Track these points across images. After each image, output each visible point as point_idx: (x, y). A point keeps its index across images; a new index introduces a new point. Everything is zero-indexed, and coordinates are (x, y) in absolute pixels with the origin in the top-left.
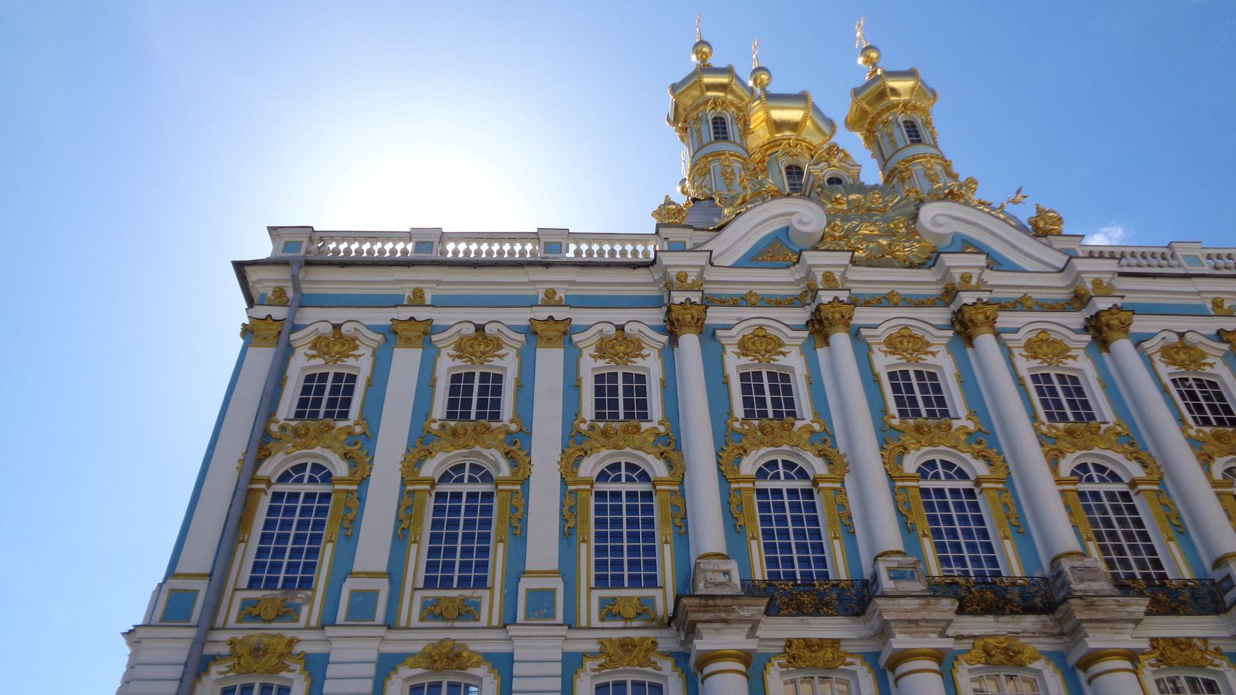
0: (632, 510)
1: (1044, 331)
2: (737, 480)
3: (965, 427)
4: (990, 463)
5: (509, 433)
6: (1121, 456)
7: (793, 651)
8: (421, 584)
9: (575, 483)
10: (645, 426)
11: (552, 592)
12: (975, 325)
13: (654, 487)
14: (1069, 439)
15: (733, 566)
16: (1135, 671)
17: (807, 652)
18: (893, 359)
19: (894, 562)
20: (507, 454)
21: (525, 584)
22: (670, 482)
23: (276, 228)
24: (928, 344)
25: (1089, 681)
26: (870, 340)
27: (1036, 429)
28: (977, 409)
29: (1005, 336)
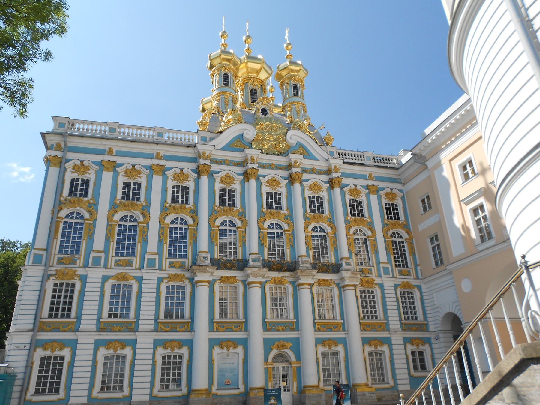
0: (181, 233)
2: (214, 227)
4: (289, 226)
5: (143, 206)
7: (223, 279)
8: (114, 255)
9: (164, 225)
10: (187, 206)
11: (155, 259)
19: (254, 256)
21: (147, 257)
23: (55, 117)
24: (280, 184)
27: (305, 215)
28: (290, 208)
29: (304, 183)
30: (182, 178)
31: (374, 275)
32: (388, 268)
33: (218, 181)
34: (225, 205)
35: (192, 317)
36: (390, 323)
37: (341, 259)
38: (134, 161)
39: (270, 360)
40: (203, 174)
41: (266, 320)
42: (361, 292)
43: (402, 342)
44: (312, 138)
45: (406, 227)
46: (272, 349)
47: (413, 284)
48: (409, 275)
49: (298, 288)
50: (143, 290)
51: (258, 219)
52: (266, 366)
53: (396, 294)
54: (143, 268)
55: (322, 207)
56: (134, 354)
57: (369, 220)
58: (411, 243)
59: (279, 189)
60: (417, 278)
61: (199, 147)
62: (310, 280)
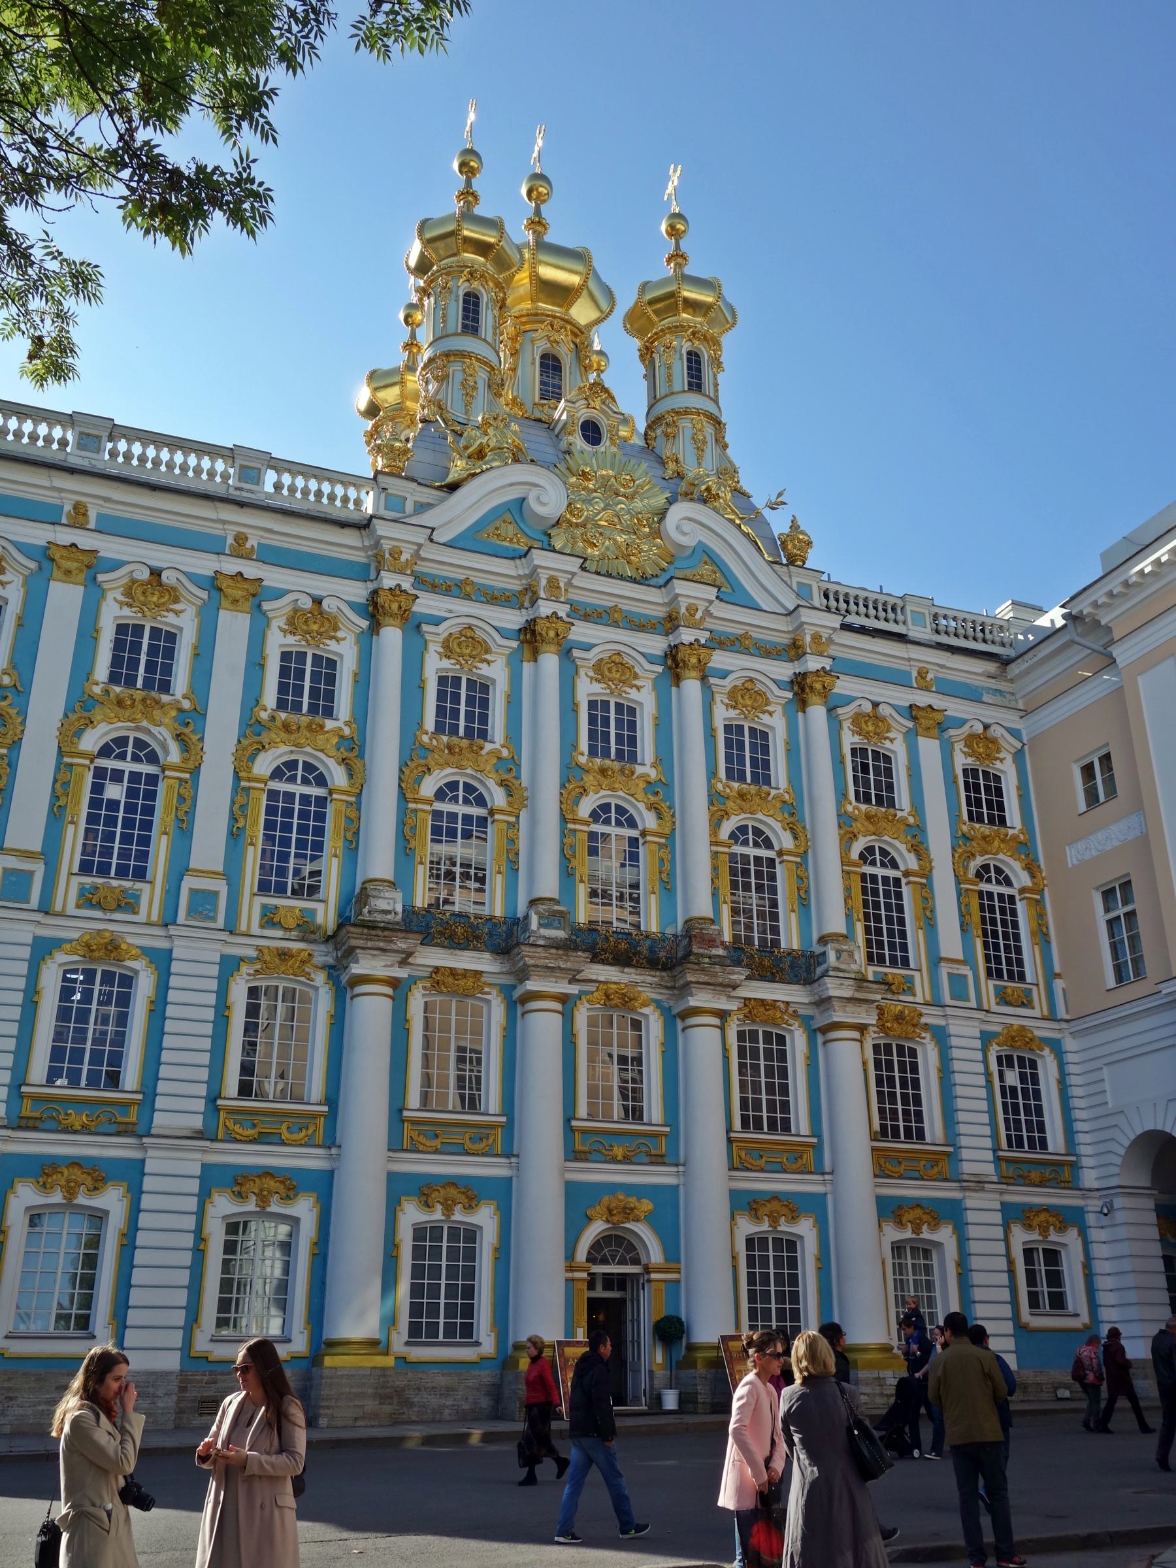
0: (304, 815)
1: (751, 680)
2: (416, 801)
4: (660, 817)
6: (779, 824)
8: (76, 869)
9: (249, 780)
10: (329, 724)
11: (216, 894)
12: (685, 666)
13: (330, 793)
15: (398, 896)
16: (722, 1029)
17: (450, 980)
18: (597, 688)
20: (178, 735)
21: (189, 883)
22: (348, 793)
24: (636, 676)
25: (684, 1030)
26: (579, 662)
27: (710, 786)
29: (712, 680)
31: (919, 998)
32: (965, 976)
33: (434, 648)
34: (454, 730)
35: (332, 1099)
36: (965, 1154)
37: (823, 940)
38: (160, 556)
39: (581, 1255)
41: (574, 1123)
43: (997, 1218)
44: (747, 535)
45: (1024, 848)
46: (590, 1219)
47: (1038, 1033)
48: (1027, 1003)
49: (680, 1025)
50: (172, 996)
51: (563, 786)
52: (570, 1275)
53: (985, 1061)
54: (175, 923)
55: (766, 765)
56: (135, 1210)
57: (911, 820)
58: (1037, 901)
59: (633, 694)
60: (1052, 1017)
61: (381, 529)
62: (723, 1004)
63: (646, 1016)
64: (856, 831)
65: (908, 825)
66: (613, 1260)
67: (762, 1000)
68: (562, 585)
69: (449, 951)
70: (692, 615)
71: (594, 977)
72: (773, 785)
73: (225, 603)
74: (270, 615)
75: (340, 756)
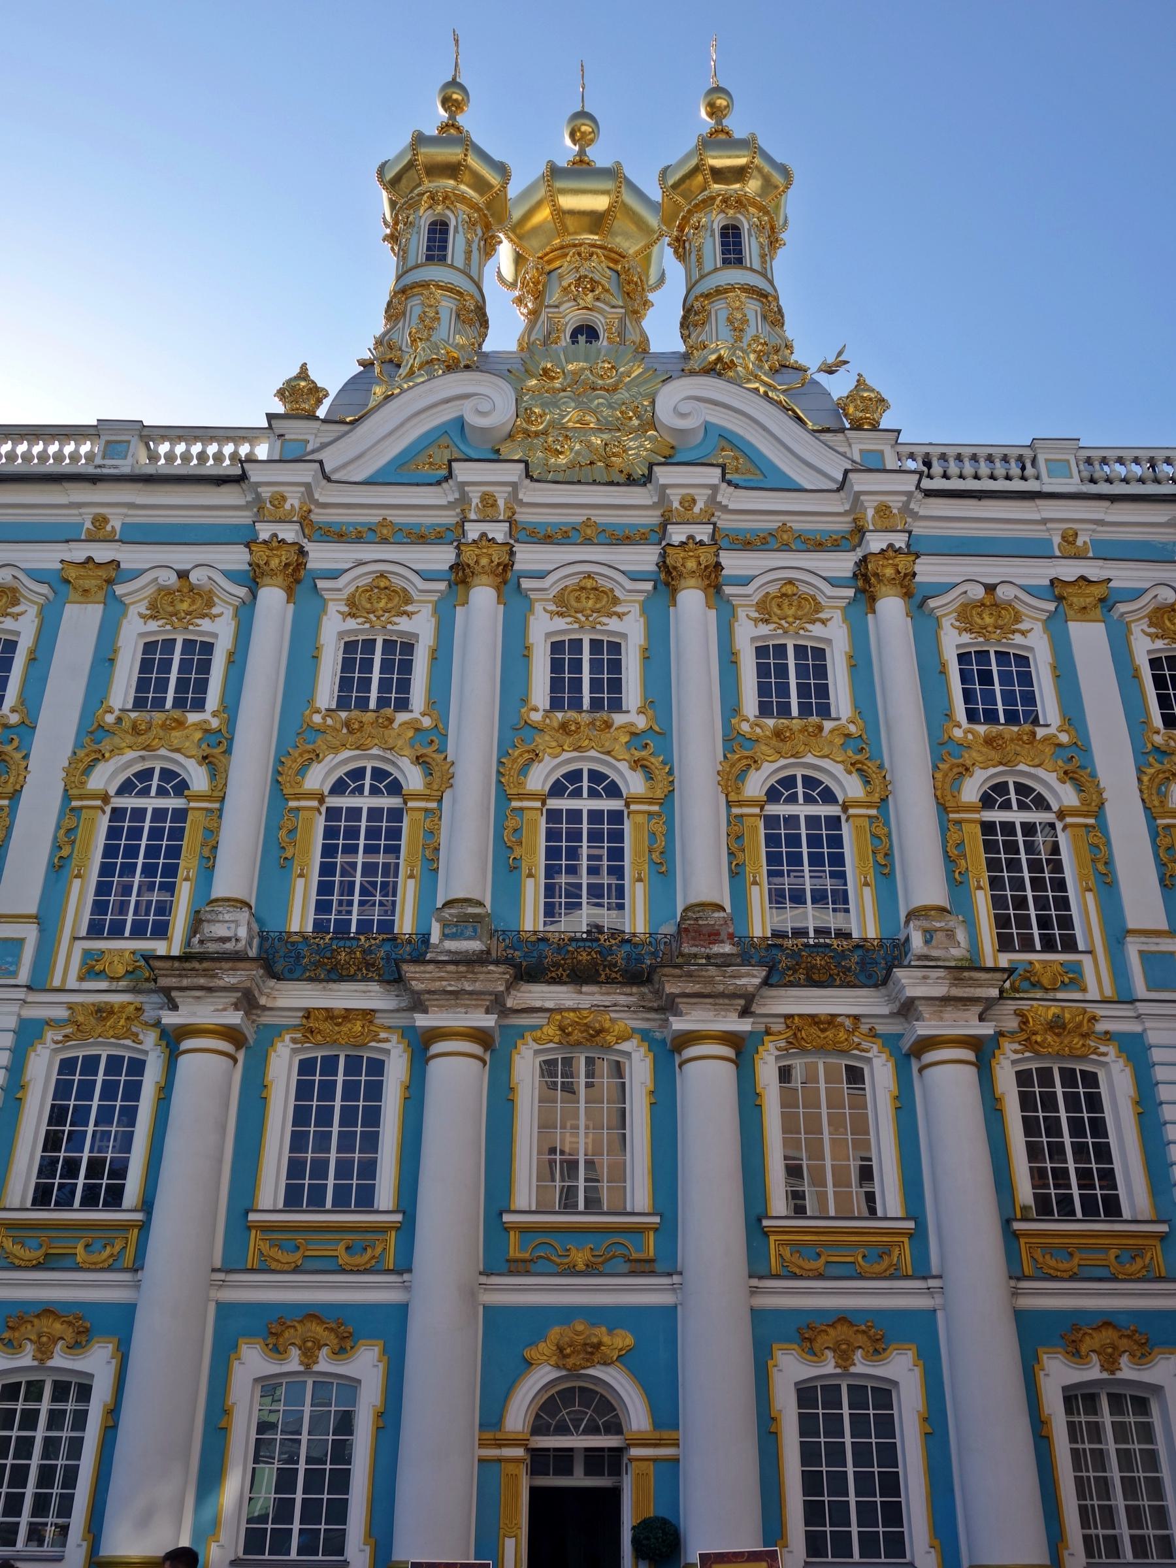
1: (790, 582)
2: (298, 797)
3: (632, 724)
4: (649, 776)
6: (841, 767)
9: (81, 797)
11: (21, 942)
14: (774, 742)
17: (327, 1026)
24: (616, 601)
28: (659, 699)
29: (728, 590)
30: (185, 606)
31: (1093, 993)
34: (363, 704)
40: (267, 580)
42: (1023, 1078)
46: (529, 1364)
63: (628, 1054)
64: (969, 763)
65: (1059, 745)
66: (577, 1427)
67: (812, 1016)
68: (501, 503)
69: (321, 986)
70: (689, 509)
71: (538, 1004)
72: (833, 715)
73: (73, 596)
74: (127, 600)
75: (201, 754)
